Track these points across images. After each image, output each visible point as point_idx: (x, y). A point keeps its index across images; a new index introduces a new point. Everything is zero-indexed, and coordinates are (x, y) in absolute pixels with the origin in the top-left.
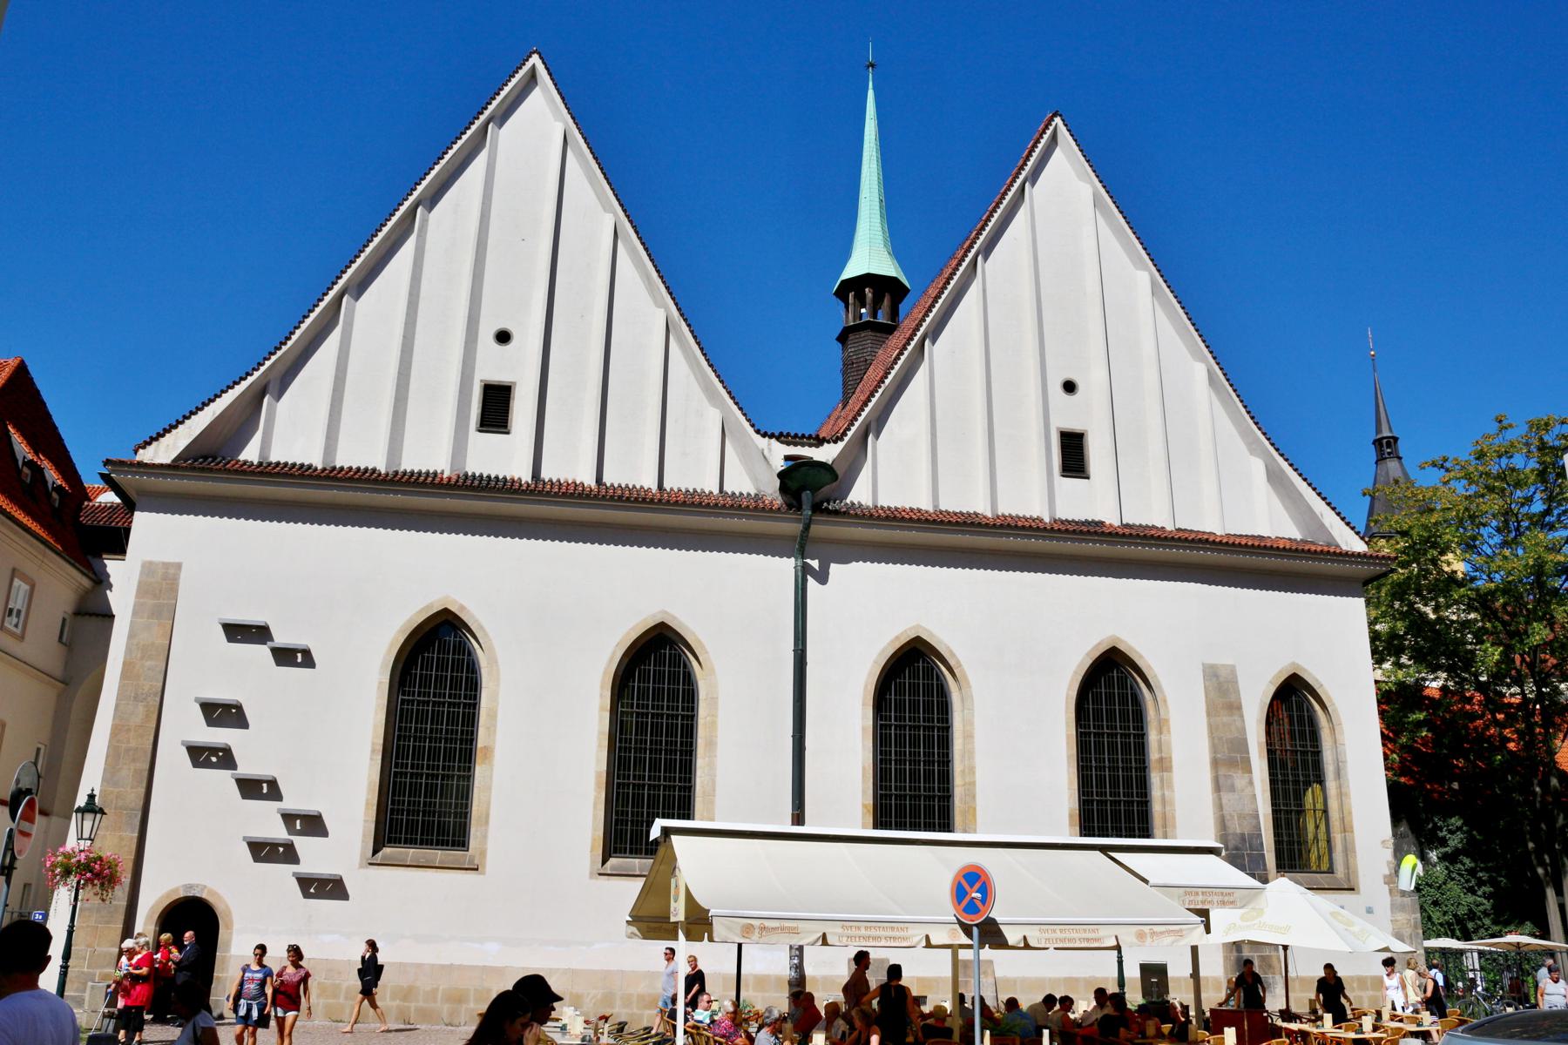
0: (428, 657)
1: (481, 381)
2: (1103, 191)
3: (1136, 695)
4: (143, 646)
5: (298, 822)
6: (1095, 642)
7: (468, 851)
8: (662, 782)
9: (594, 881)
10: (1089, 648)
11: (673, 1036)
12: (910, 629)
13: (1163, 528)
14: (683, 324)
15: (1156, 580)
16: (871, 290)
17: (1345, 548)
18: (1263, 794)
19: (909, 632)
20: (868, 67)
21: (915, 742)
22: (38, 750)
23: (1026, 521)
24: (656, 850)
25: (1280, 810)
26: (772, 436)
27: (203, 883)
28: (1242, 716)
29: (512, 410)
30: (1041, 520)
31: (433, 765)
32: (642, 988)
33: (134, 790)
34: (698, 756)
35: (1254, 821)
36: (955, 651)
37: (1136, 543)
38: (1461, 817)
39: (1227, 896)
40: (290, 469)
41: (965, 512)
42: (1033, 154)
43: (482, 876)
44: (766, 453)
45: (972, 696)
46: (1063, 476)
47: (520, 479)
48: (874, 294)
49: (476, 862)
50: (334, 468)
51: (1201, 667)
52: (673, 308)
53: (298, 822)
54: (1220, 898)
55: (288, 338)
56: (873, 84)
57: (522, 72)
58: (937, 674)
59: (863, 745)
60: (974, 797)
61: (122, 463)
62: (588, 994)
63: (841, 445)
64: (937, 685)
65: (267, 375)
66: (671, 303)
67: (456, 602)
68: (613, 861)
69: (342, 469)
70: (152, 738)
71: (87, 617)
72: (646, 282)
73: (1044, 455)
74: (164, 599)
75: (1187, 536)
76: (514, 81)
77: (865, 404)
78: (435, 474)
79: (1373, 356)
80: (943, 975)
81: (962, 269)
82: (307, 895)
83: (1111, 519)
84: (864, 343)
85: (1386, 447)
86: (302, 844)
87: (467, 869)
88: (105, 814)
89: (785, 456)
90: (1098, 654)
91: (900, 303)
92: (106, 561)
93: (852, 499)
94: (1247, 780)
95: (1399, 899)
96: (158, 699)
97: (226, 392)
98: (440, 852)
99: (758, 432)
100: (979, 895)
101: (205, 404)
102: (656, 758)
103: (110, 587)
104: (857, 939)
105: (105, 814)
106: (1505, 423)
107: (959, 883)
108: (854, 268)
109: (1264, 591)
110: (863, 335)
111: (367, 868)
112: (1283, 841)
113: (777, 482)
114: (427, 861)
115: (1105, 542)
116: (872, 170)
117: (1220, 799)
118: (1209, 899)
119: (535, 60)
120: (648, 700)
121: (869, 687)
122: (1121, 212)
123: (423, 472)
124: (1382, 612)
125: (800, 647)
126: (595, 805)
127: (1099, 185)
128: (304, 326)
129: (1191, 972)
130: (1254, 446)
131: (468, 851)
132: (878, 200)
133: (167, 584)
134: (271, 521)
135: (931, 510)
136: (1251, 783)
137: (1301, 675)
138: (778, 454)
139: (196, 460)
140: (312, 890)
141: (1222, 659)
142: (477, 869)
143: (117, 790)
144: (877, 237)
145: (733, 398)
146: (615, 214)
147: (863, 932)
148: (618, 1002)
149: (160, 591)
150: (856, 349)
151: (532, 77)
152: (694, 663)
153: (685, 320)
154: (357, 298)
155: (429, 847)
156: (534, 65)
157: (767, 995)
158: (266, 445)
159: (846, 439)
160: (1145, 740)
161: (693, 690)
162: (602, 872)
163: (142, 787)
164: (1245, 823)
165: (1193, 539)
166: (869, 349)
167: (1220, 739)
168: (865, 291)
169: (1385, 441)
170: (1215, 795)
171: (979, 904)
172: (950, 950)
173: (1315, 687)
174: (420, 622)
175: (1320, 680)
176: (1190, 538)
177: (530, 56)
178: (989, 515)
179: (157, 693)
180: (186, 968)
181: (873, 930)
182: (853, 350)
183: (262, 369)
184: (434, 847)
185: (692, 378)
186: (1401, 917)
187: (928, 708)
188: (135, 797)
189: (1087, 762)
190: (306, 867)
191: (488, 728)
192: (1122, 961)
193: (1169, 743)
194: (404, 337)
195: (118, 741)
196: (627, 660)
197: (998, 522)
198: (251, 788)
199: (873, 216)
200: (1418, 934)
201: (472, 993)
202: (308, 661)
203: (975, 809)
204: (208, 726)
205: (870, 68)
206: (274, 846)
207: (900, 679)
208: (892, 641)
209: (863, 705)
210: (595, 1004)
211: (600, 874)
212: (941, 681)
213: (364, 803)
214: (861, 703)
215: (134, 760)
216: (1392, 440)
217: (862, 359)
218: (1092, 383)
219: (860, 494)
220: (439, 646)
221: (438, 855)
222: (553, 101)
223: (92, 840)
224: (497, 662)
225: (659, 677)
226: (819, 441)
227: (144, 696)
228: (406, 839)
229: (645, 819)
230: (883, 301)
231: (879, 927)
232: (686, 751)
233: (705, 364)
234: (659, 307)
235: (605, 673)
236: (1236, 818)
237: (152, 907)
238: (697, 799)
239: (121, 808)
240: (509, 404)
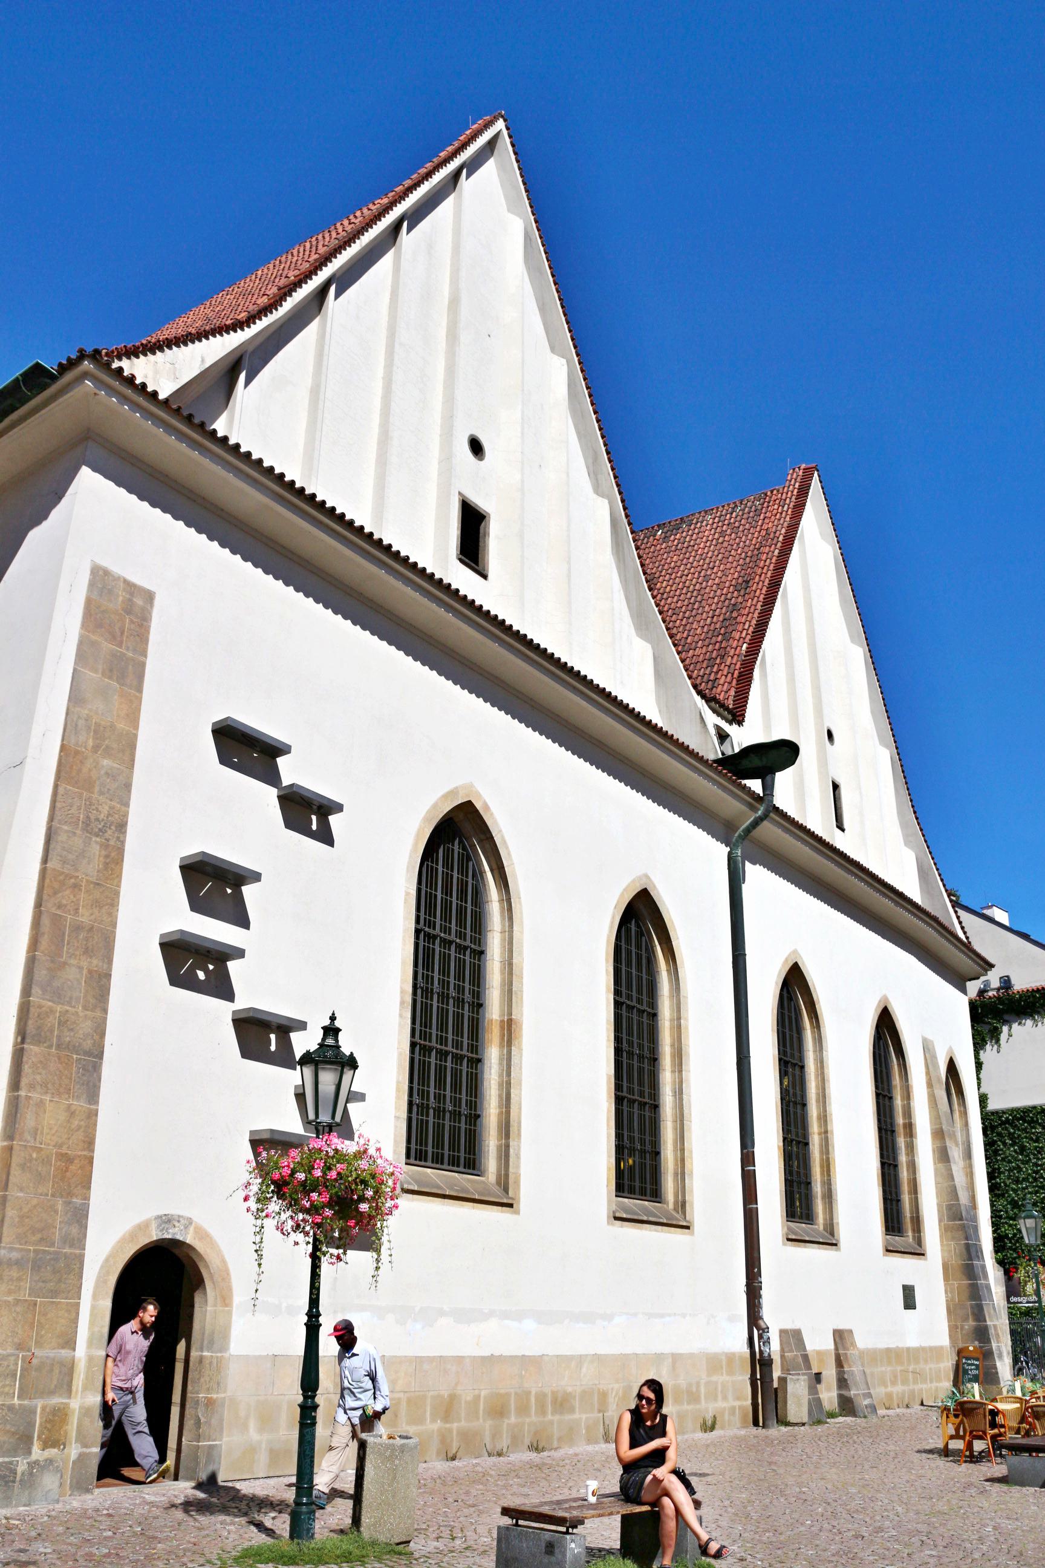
27: (186, 1214)
143: (59, 1008)
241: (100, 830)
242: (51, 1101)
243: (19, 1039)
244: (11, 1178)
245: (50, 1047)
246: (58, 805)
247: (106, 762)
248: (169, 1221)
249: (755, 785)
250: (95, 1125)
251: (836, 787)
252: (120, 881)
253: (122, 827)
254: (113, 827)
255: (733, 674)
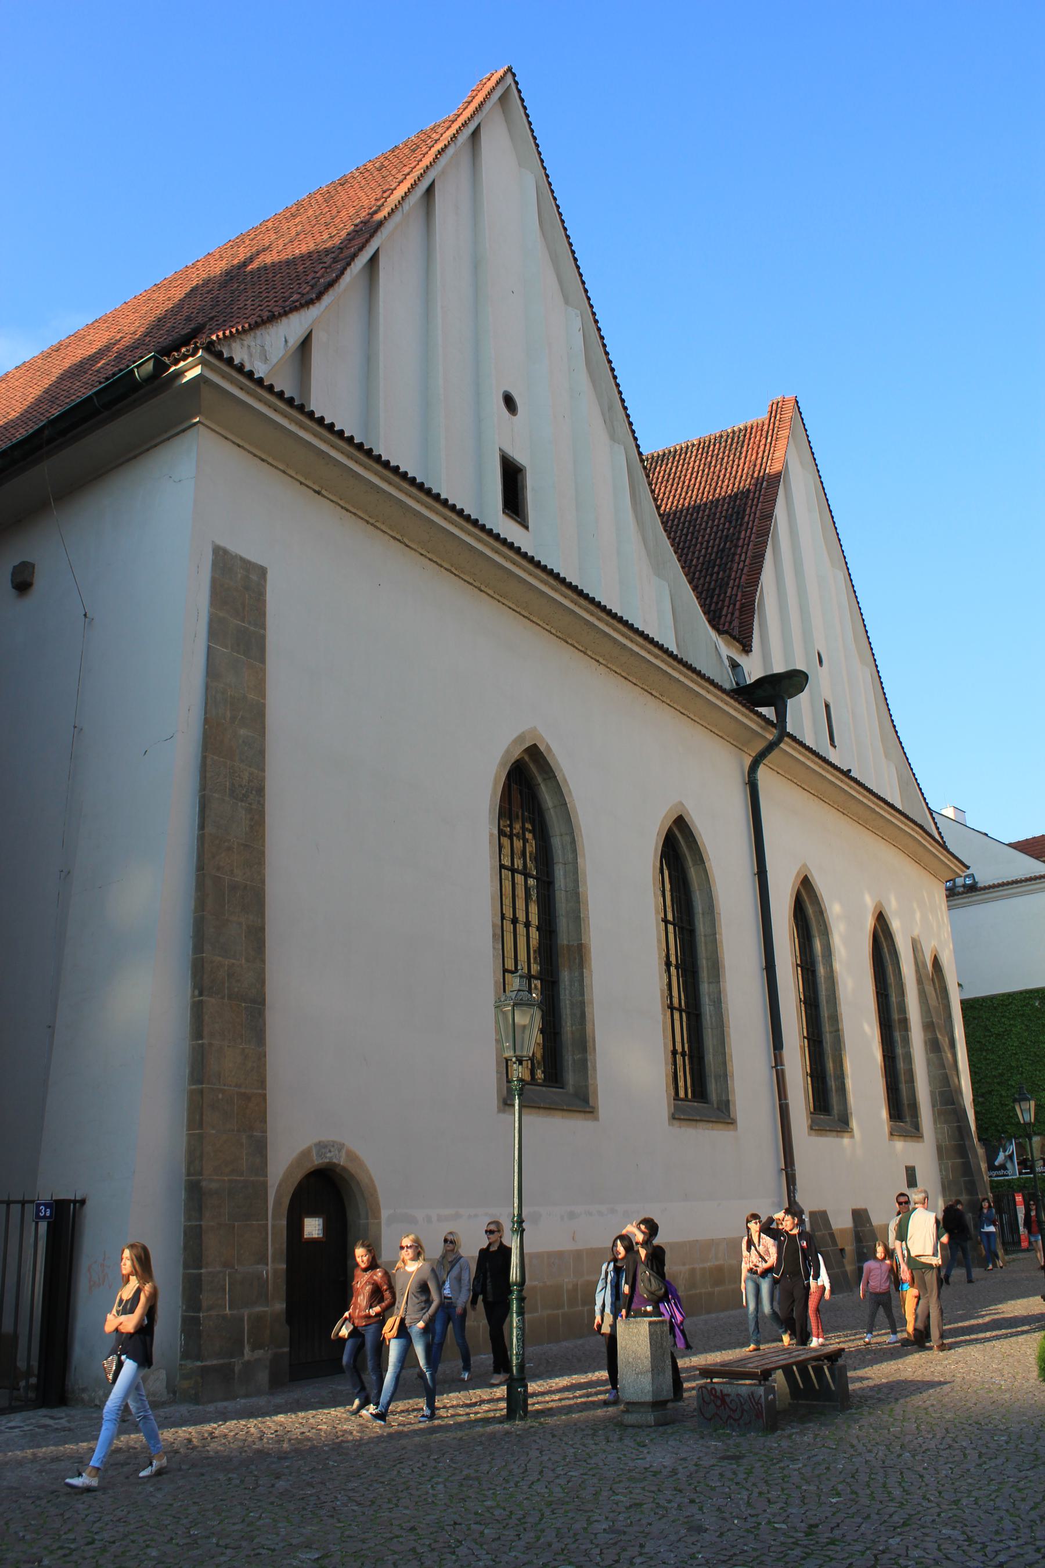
241: (244, 795)
242: (229, 1046)
243: (197, 992)
244: (204, 1117)
245: (223, 998)
246: (208, 775)
247: (242, 732)
248: (325, 1147)
249: (768, 712)
250: (265, 1065)
251: (827, 706)
252: (264, 841)
253: (261, 791)
254: (254, 792)
255: (735, 605)
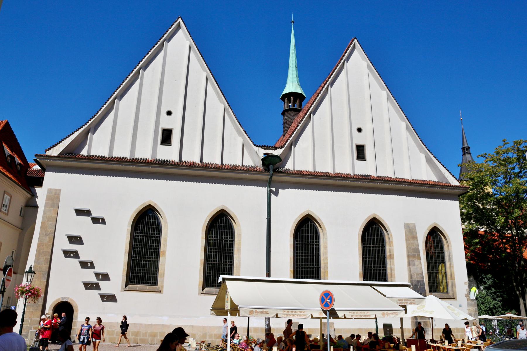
0: (144, 221)
1: (162, 128)
2: (371, 64)
3: (382, 233)
4: (48, 217)
5: (100, 276)
6: (368, 216)
7: (157, 286)
8: (222, 263)
9: (200, 296)
10: (366, 218)
11: (226, 348)
12: (306, 211)
13: (391, 177)
14: (230, 109)
15: (388, 195)
16: (293, 98)
17: (452, 184)
18: (424, 267)
19: (305, 212)
20: (292, 23)
21: (307, 249)
22: (13, 252)
23: (345, 175)
24: (221, 285)
25: (430, 272)
26: (259, 146)
28: (417, 241)
29: (172, 138)
30: (350, 175)
31: (146, 257)
32: (216, 332)
33: (45, 265)
34: (235, 254)
35: (422, 276)
36: (321, 219)
37: (382, 182)
38: (491, 274)
39: (412, 301)
40: (98, 158)
41: (324, 172)
42: (347, 52)
43: (162, 294)
44: (257, 152)
45: (327, 234)
46: (357, 160)
47: (175, 161)
48: (294, 99)
49: (160, 290)
50: (112, 157)
51: (404, 224)
52: (226, 104)
53: (100, 276)
54: (410, 302)
55: (97, 114)
56: (293, 28)
57: (175, 24)
58: (315, 226)
59: (290, 250)
60: (327, 268)
61: (41, 156)
62: (198, 334)
63: (283, 149)
64: (315, 230)
65: (90, 126)
66: (225, 102)
67: (153, 202)
68: (206, 289)
69: (115, 157)
70: (51, 248)
71: (29, 207)
72: (217, 95)
73: (351, 153)
74: (55, 201)
75: (399, 180)
76: (173, 27)
77: (291, 136)
78: (146, 159)
79: (462, 119)
80: (317, 328)
81: (323, 90)
82: (103, 301)
83: (374, 174)
84: (290, 115)
85: (466, 150)
86: (102, 283)
87: (157, 292)
88: (35, 273)
89: (264, 153)
90: (369, 220)
91: (303, 102)
92: (35, 189)
93: (286, 168)
94: (419, 262)
95: (470, 302)
96: (53, 235)
97: (76, 132)
98: (148, 286)
99: (255, 145)
100: (329, 301)
101: (69, 136)
102: (220, 255)
103: (37, 197)
104: (288, 315)
105: (35, 273)
106: (506, 142)
107: (322, 297)
108: (287, 90)
109: (425, 199)
110: (290, 112)
111: (123, 291)
112: (431, 282)
113: (261, 162)
114: (143, 289)
115: (371, 182)
116: (293, 57)
117: (410, 268)
118: (406, 302)
119: (180, 20)
120: (218, 235)
121: (292, 231)
122: (377, 71)
123: (142, 158)
124: (465, 205)
125: (269, 217)
126: (200, 270)
127: (369, 62)
128: (102, 110)
129: (400, 326)
130: (421, 150)
131: (157, 286)
132: (295, 67)
133: (56, 196)
134: (91, 175)
135: (313, 171)
136: (420, 263)
137: (437, 227)
138: (261, 152)
139: (66, 155)
140: (105, 299)
141: (411, 221)
142: (160, 292)
144: (295, 80)
145: (246, 134)
146: (207, 72)
147: (290, 313)
148: (208, 337)
149: (54, 198)
150: (288, 117)
151: (179, 26)
152: (233, 223)
153: (230, 108)
154: (120, 100)
155: (144, 284)
156: (179, 22)
157: (258, 334)
158: (89, 150)
159: (284, 147)
160: (385, 249)
161: (233, 232)
162: (202, 293)
163: (48, 264)
164: (419, 276)
165: (401, 181)
166: (292, 117)
167: (410, 248)
168: (291, 98)
169: (465, 148)
170: (408, 267)
171: (329, 304)
172: (319, 319)
173: (442, 231)
174: (141, 209)
175: (444, 228)
176: (400, 181)
177: (178, 19)
178: (333, 173)
179: (53, 233)
180: (62, 325)
181: (293, 312)
182: (287, 117)
183: (88, 124)
184: (146, 284)
185: (233, 127)
186: (471, 308)
187: (312, 238)
188: (45, 268)
189: (365, 256)
190: (103, 291)
191: (164, 245)
192: (377, 323)
193: (393, 250)
194: (136, 113)
195: (40, 249)
196: (211, 222)
197: (336, 175)
198: (84, 265)
199: (293, 72)
200: (477, 314)
201: (159, 333)
202: (104, 222)
203: (328, 272)
204: (70, 244)
205: (293, 23)
206: (92, 284)
207: (303, 228)
208: (300, 215)
209: (290, 237)
210: (200, 337)
211: (202, 294)
212: (316, 229)
213: (122, 270)
214: (289, 236)
215: (45, 255)
216: (468, 148)
217: (290, 121)
218: (367, 129)
219: (289, 166)
220: (148, 217)
221: (147, 287)
222: (186, 34)
223: (31, 282)
224: (167, 222)
225: (221, 227)
226: (275, 148)
227: (48, 234)
228: (136, 282)
229: (217, 275)
230: (297, 101)
231: (296, 311)
232: (231, 252)
233: (237, 122)
234: (222, 103)
235: (203, 226)
236: (415, 275)
237: (51, 305)
238: (234, 268)
239: (41, 271)
240: (171, 136)
